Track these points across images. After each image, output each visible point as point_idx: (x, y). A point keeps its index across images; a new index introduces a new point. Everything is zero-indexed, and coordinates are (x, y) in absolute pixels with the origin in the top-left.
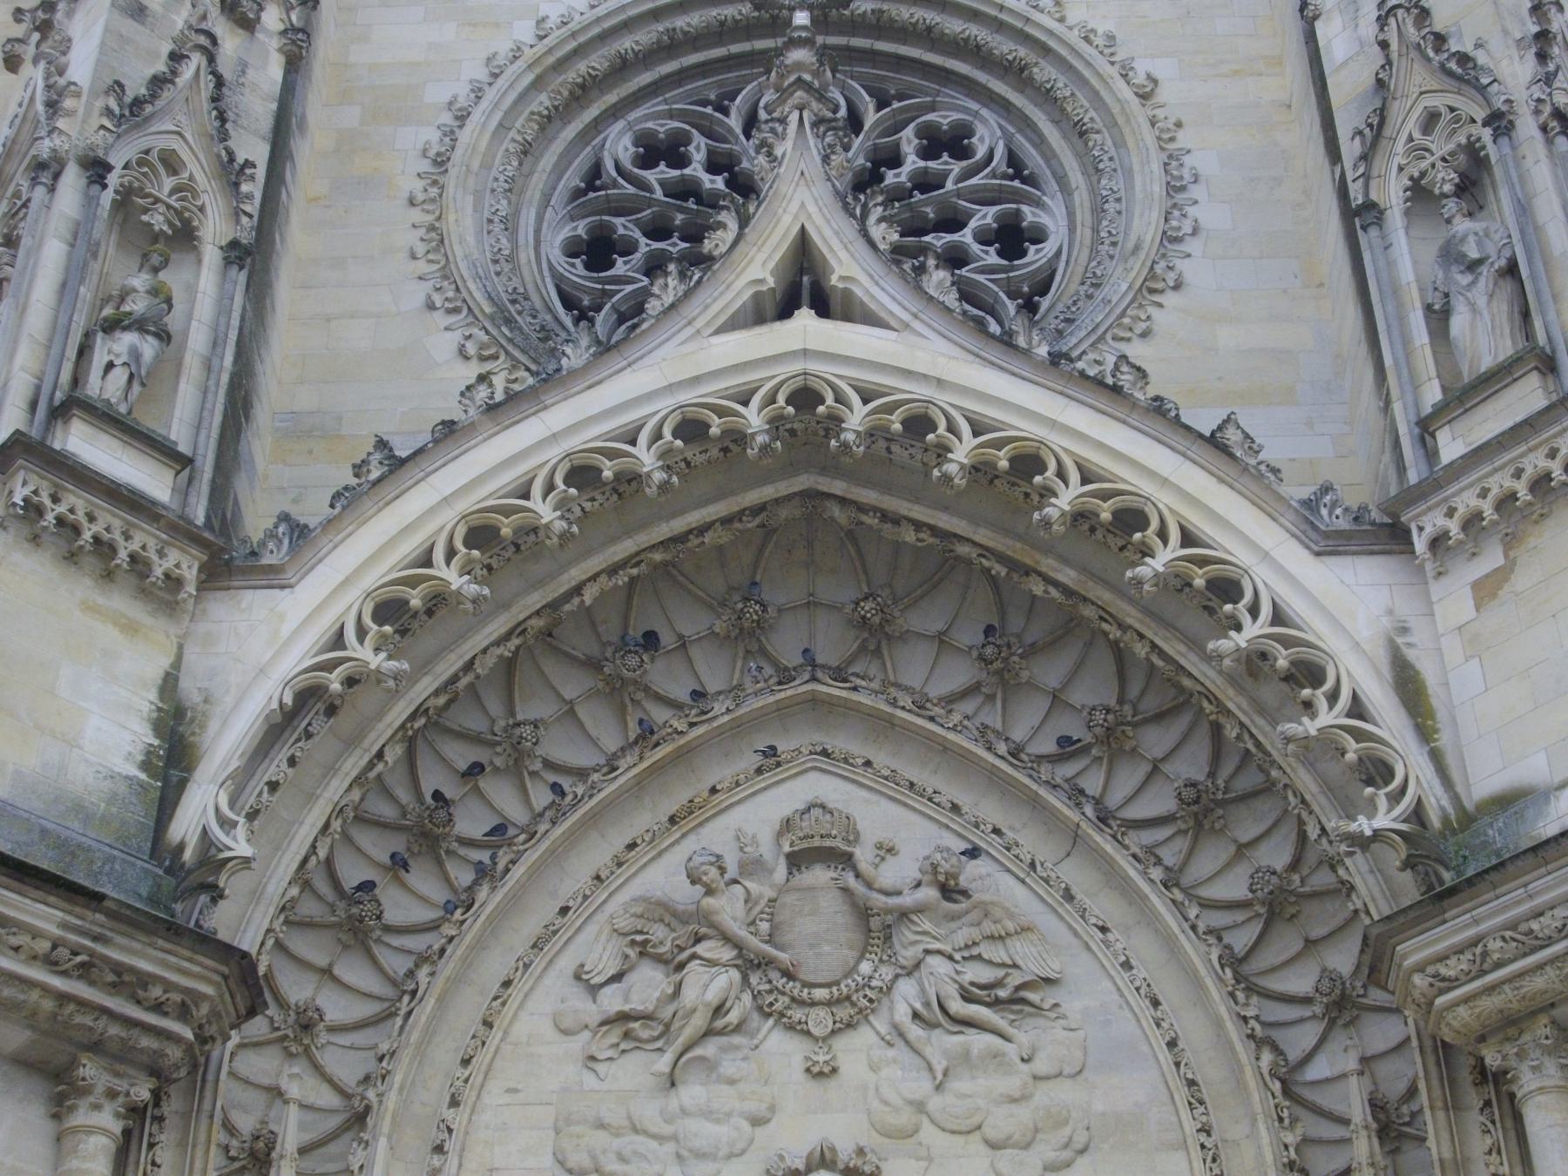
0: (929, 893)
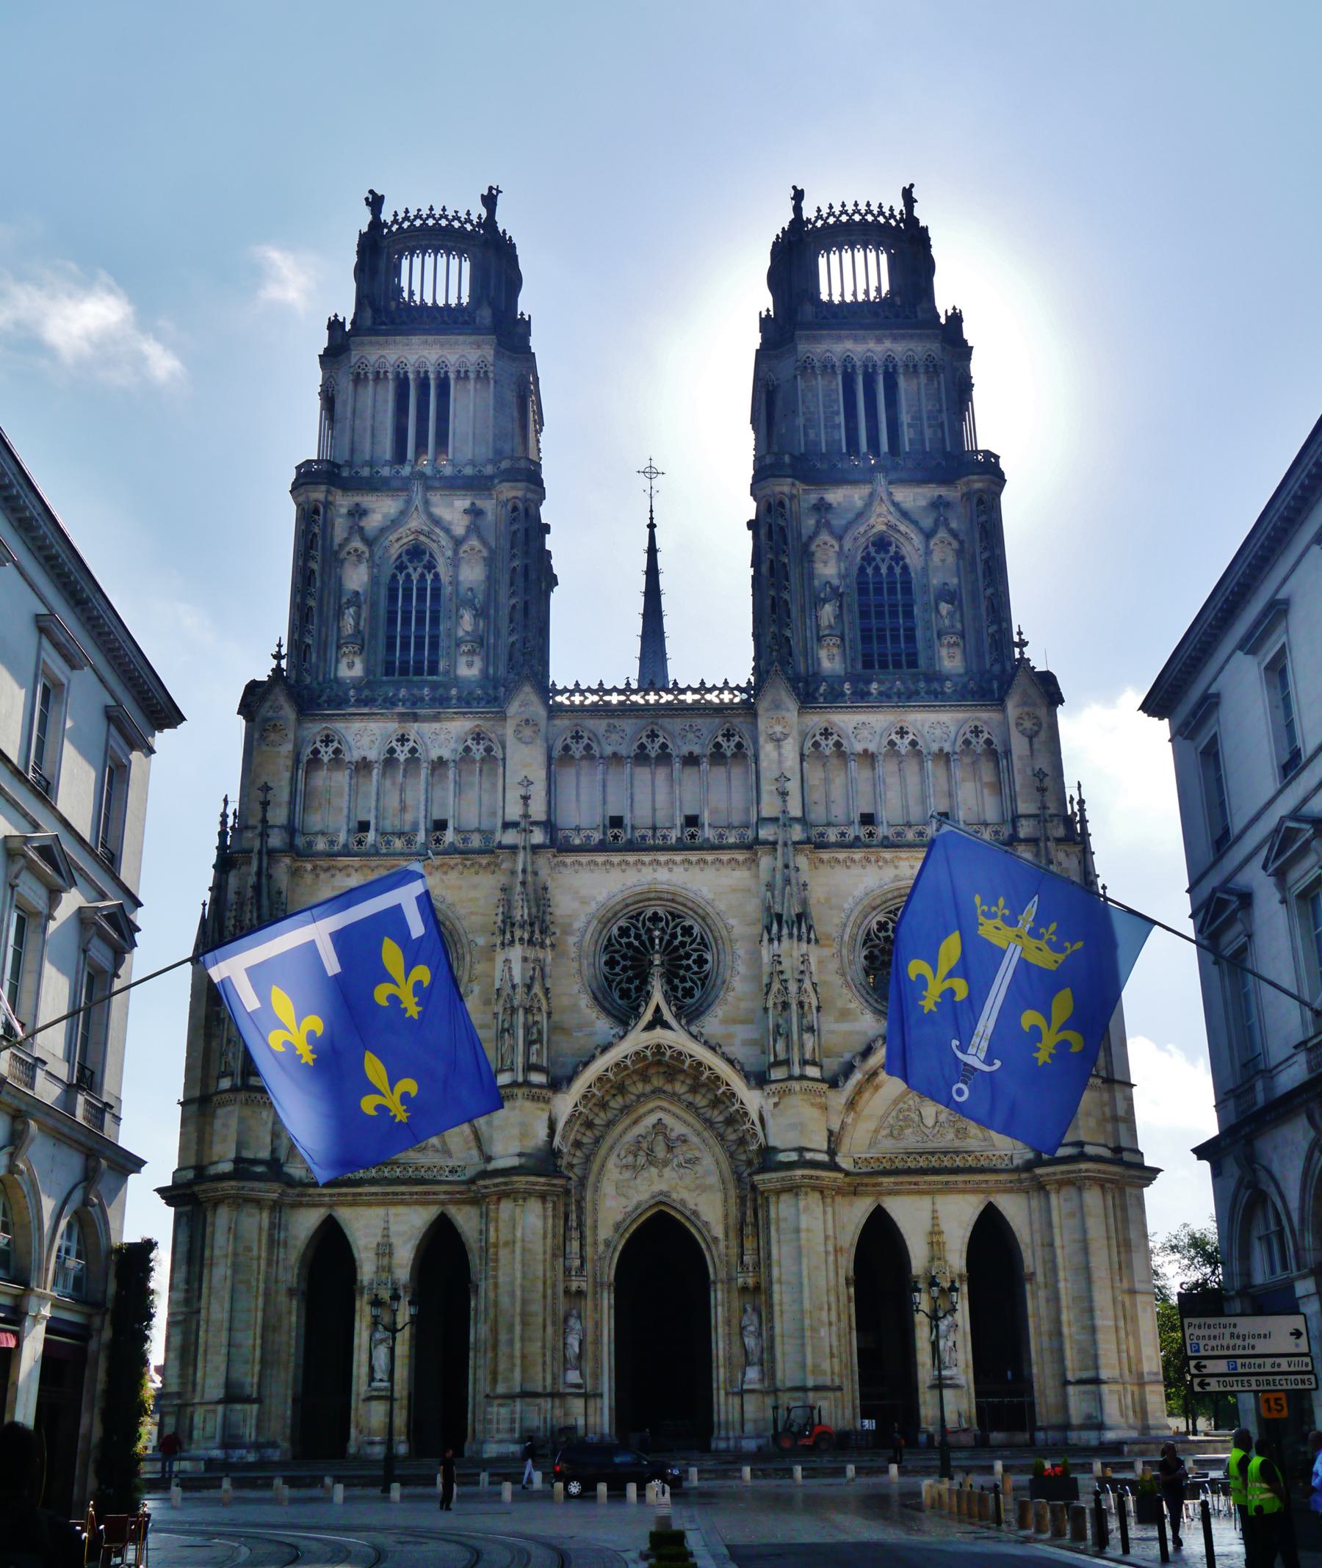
0: (679, 1143)
